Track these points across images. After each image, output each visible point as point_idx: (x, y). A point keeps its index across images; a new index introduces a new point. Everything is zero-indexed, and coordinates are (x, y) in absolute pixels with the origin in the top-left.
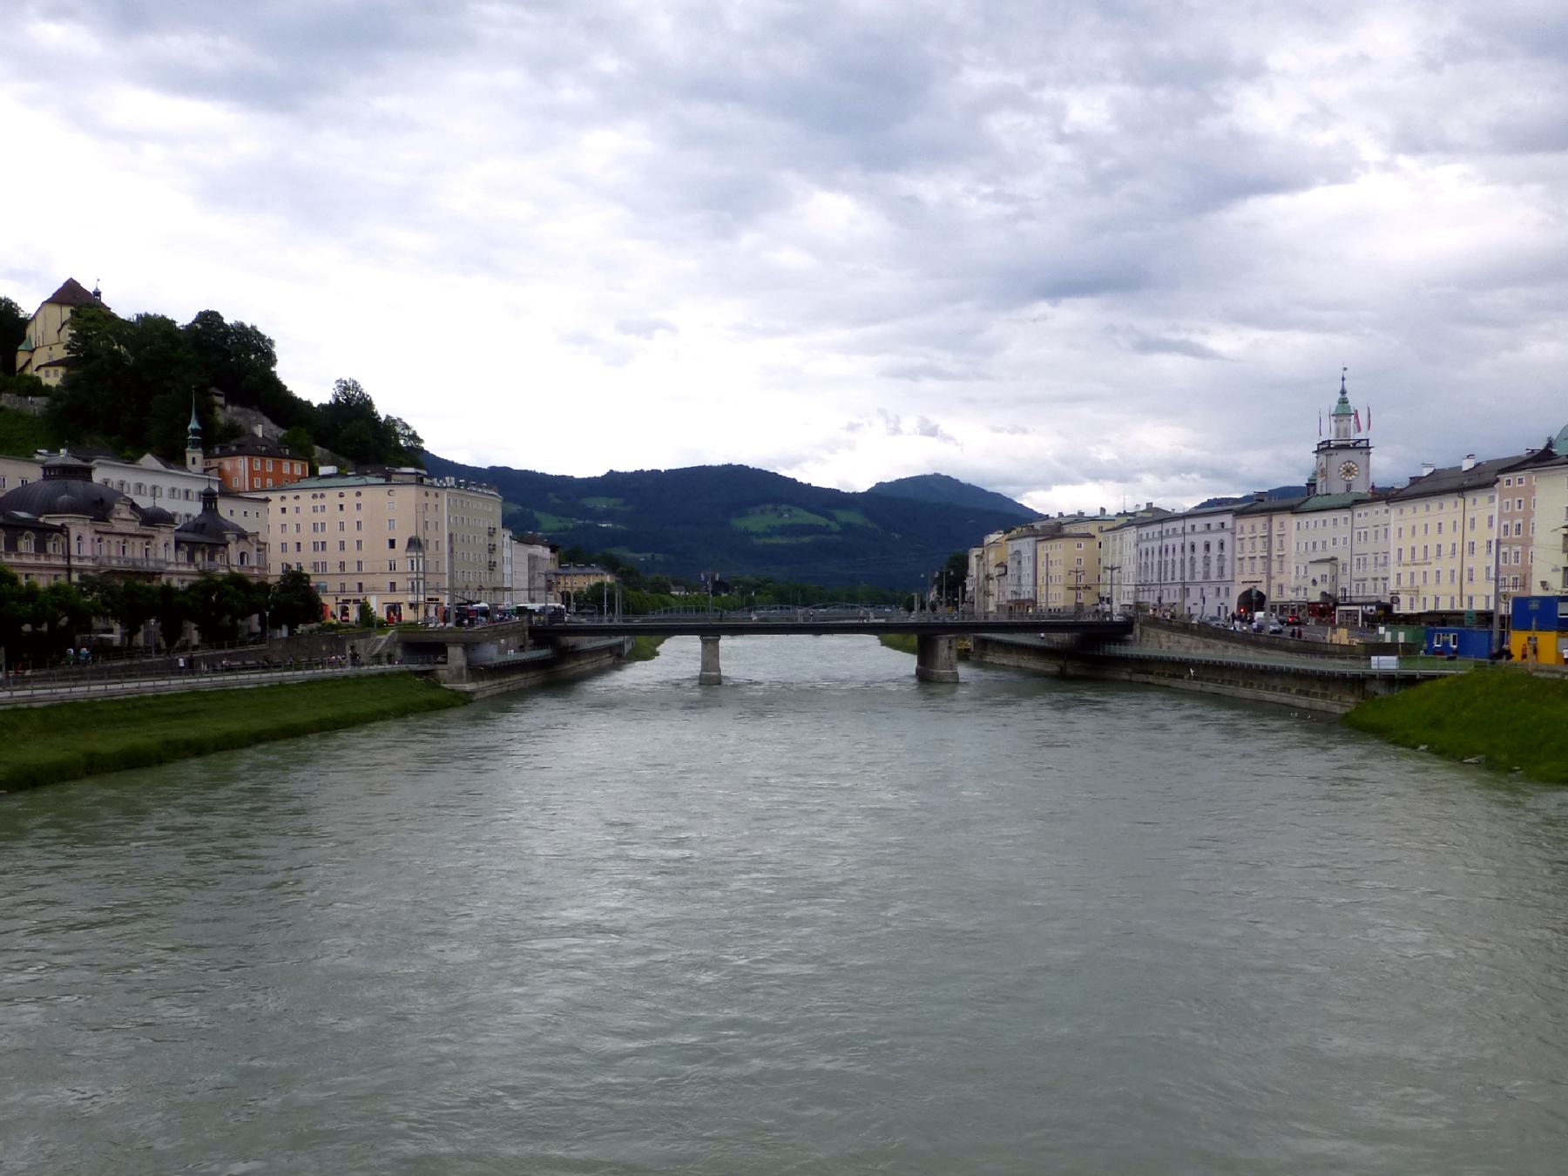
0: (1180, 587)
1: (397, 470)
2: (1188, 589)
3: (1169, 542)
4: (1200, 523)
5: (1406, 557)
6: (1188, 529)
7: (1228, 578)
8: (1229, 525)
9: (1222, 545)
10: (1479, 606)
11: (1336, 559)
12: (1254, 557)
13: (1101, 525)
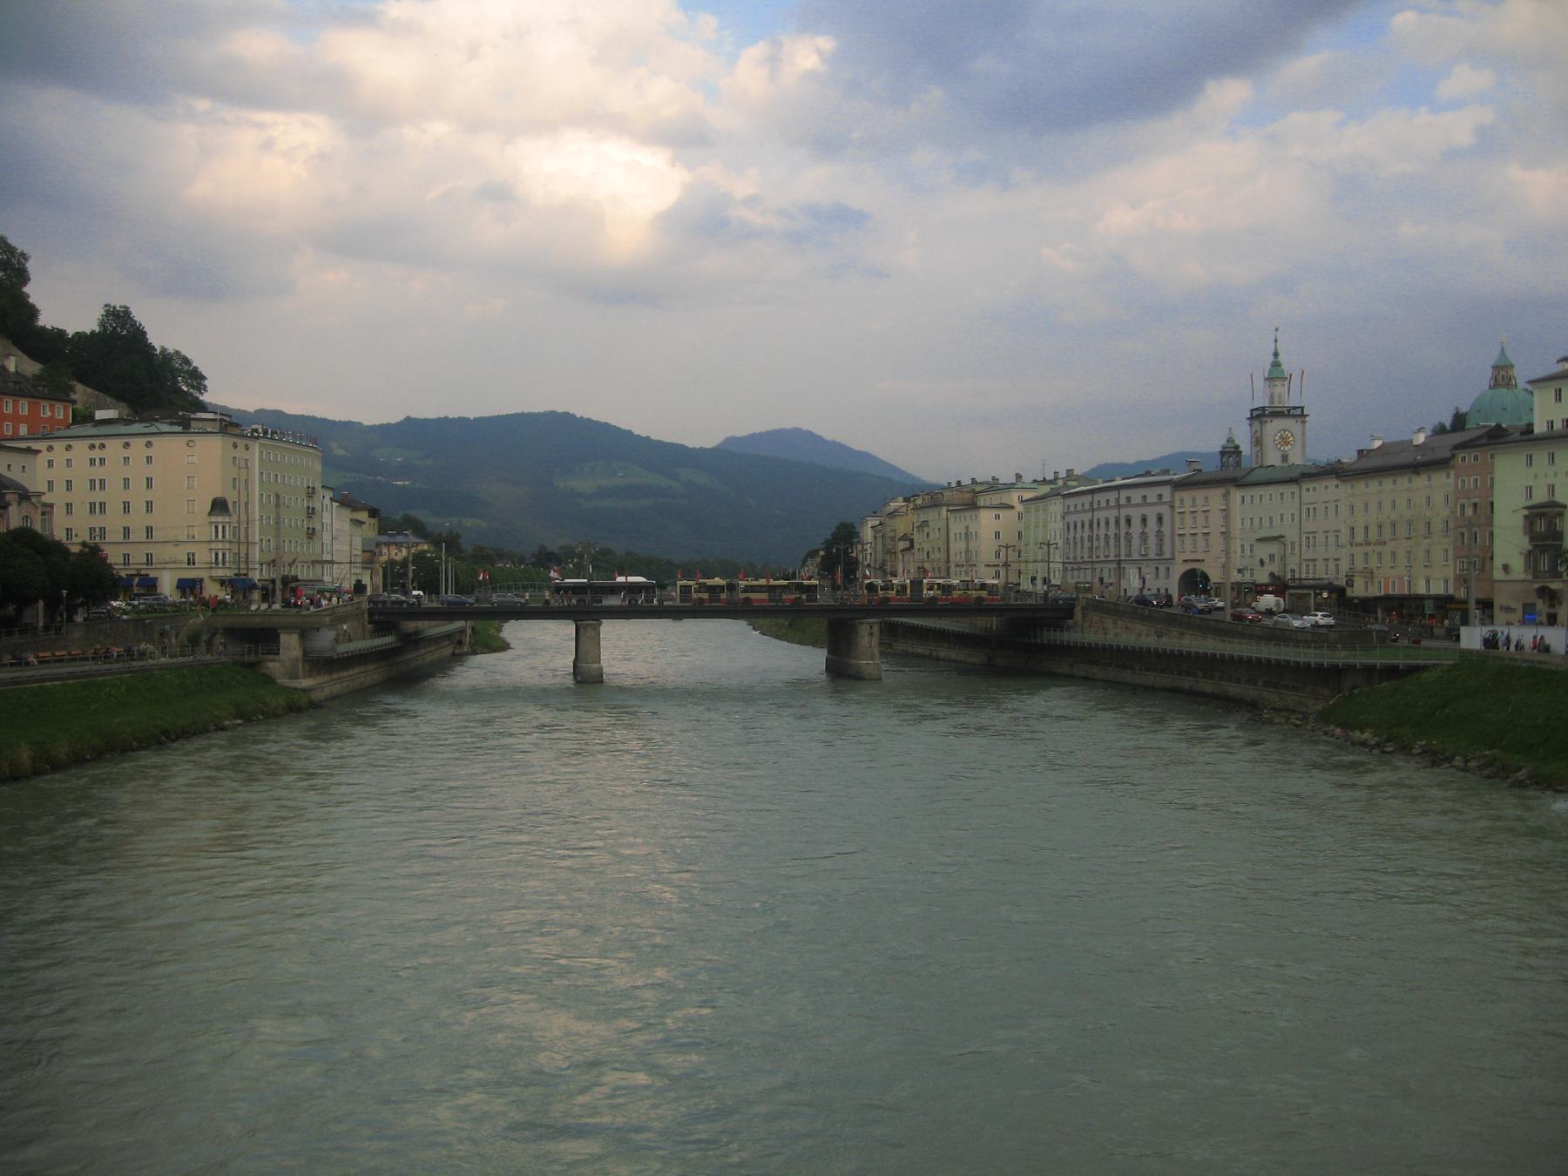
0: (1115, 565)
1: (192, 416)
2: (1124, 568)
3: (1101, 515)
4: (1136, 496)
5: (1360, 537)
6: (1123, 501)
7: (1168, 556)
8: (1166, 498)
9: (1160, 519)
10: (1438, 589)
11: (1283, 537)
12: (1196, 534)
13: (1021, 494)
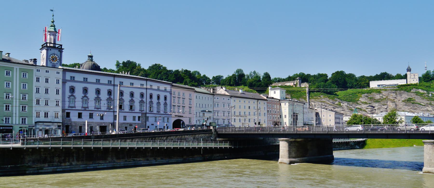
9: (165, 98)
12: (180, 106)
